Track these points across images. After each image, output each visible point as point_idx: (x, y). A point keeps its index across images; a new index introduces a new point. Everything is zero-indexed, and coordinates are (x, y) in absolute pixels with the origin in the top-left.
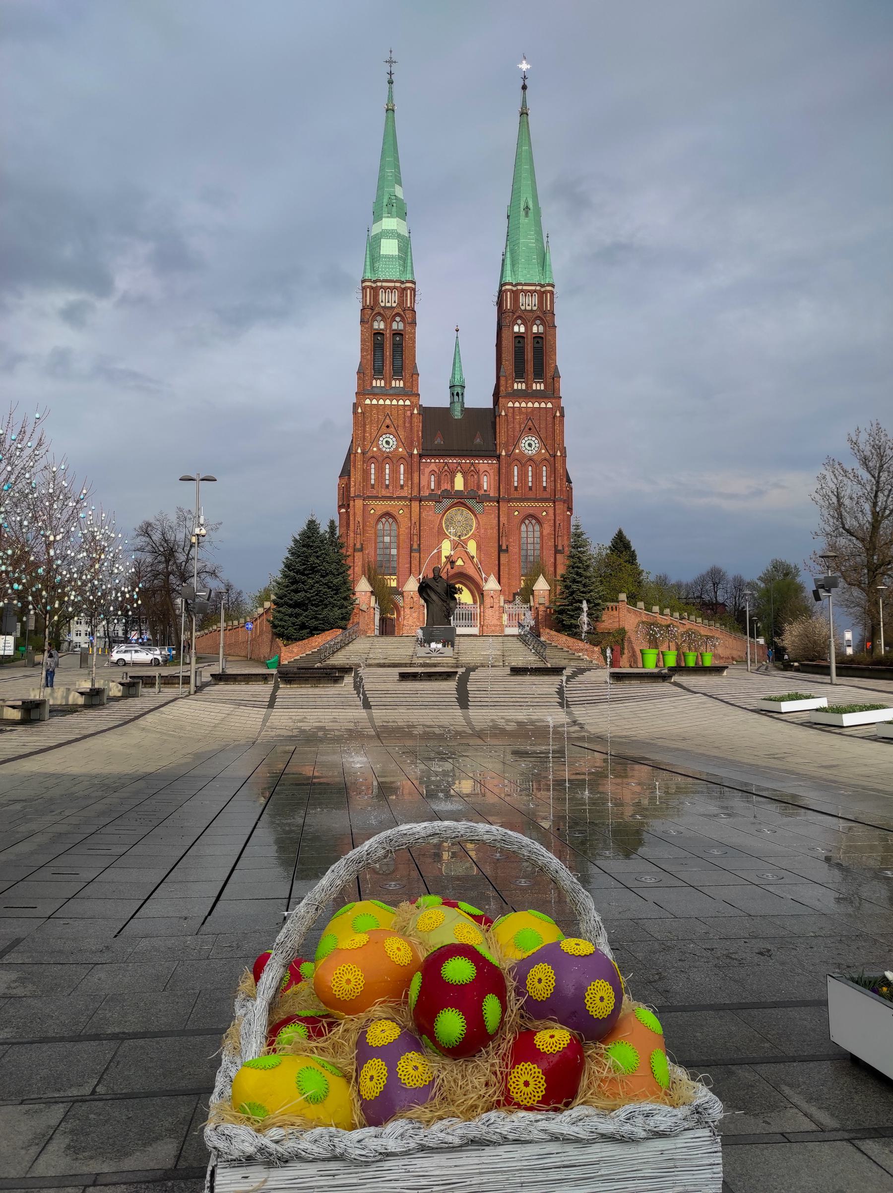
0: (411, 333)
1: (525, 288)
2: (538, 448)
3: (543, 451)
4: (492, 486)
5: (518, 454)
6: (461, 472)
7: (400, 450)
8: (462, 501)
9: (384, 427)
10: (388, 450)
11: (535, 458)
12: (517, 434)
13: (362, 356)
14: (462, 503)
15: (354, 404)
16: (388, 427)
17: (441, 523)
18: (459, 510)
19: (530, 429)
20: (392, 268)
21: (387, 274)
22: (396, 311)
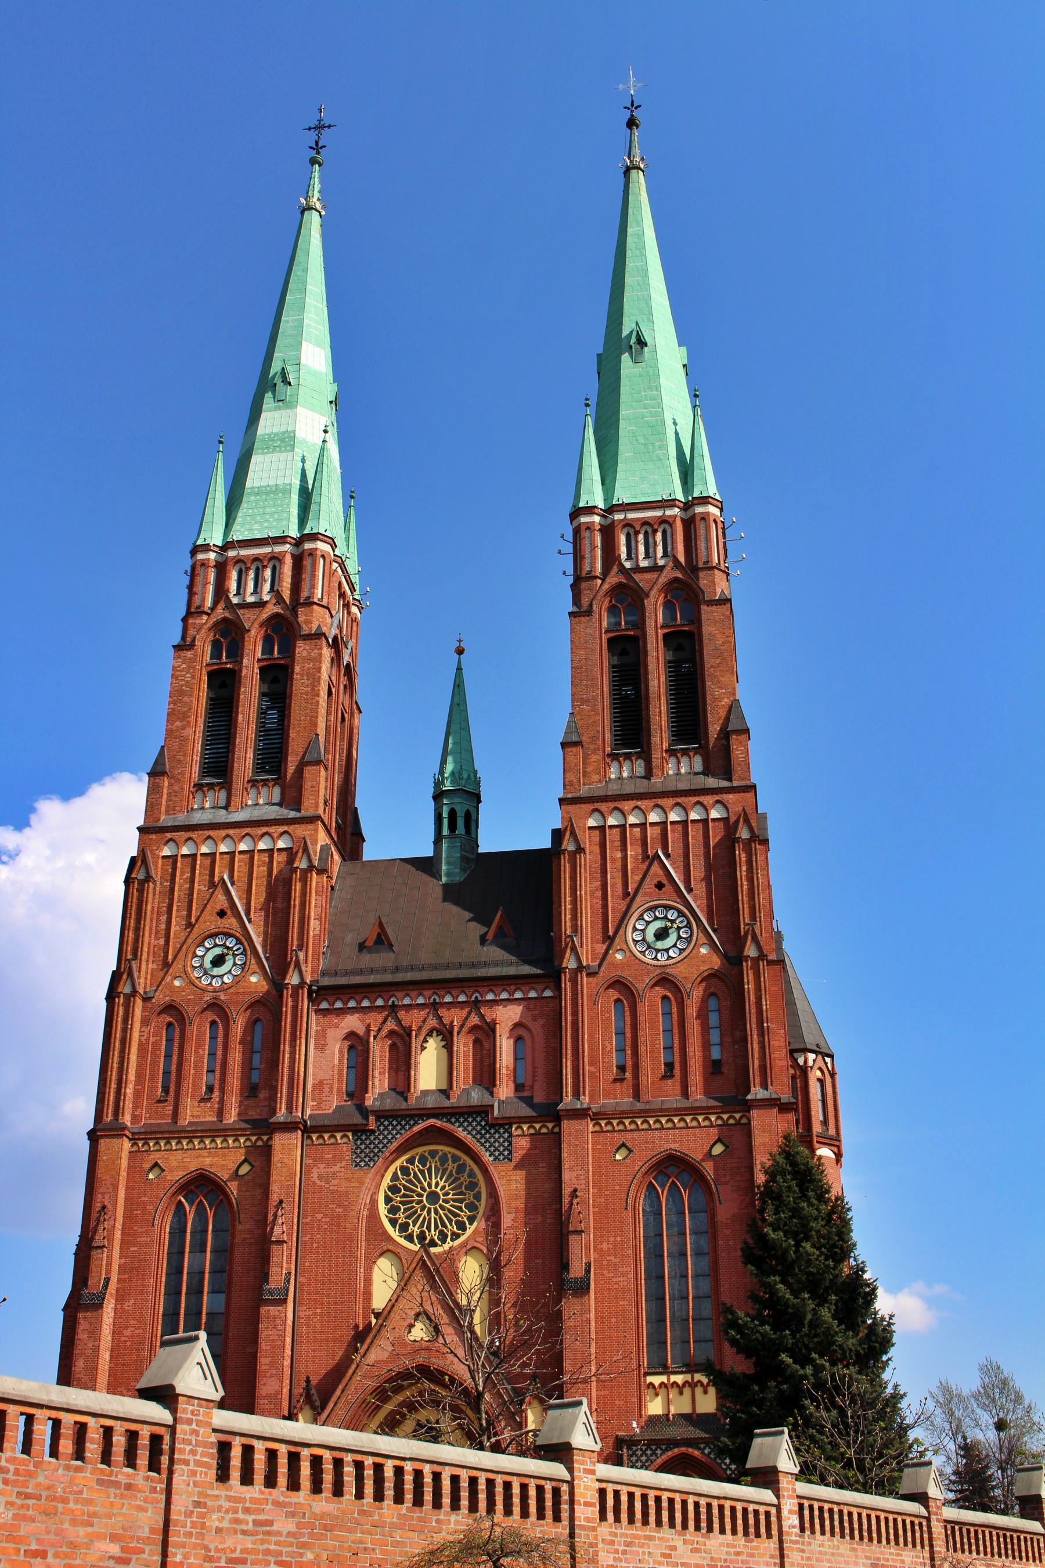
0: (310, 660)
1: (631, 516)
2: (689, 940)
3: (703, 951)
4: (540, 1071)
5: (623, 965)
6: (439, 1033)
7: (254, 979)
8: (439, 1123)
9: (210, 915)
10: (216, 983)
11: (679, 973)
12: (615, 904)
13: (170, 733)
14: (441, 1131)
15: (133, 860)
16: (222, 914)
17: (374, 1203)
18: (433, 1154)
19: (660, 886)
20: (272, 514)
21: (256, 526)
22: (272, 609)
